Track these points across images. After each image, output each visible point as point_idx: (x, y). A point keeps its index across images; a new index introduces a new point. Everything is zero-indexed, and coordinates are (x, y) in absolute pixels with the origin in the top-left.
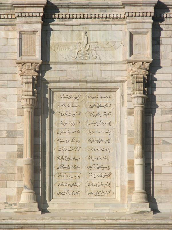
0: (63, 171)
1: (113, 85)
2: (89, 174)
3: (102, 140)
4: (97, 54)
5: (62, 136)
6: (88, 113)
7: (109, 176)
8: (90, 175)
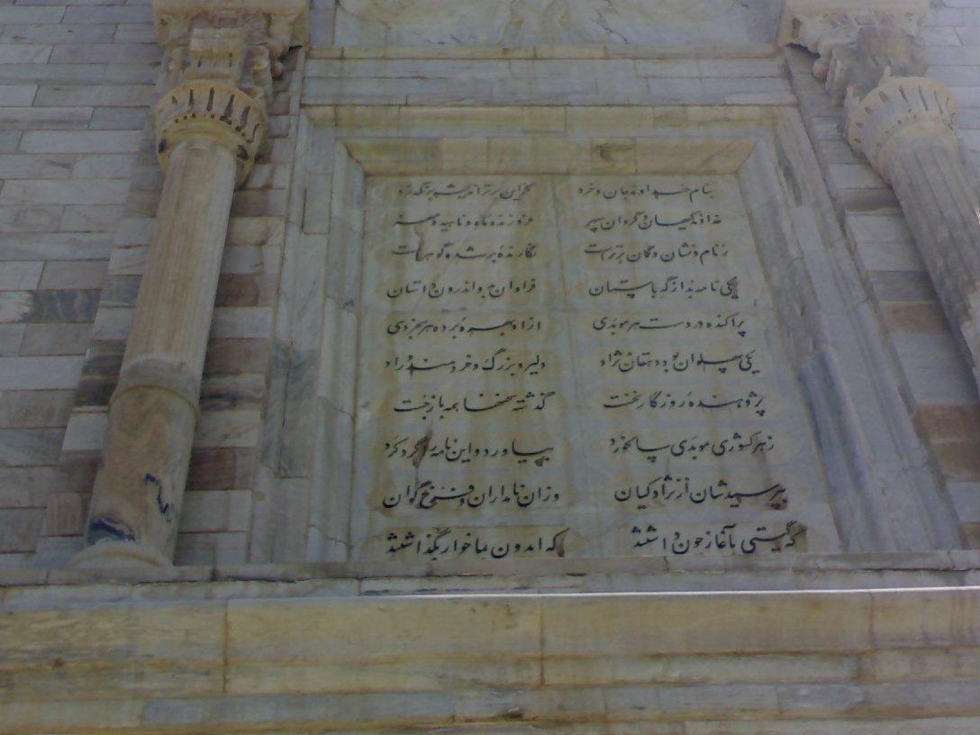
0: (426, 522)
2: (635, 530)
3: (697, 358)
4: (611, 31)
5: (419, 347)
6: (584, 247)
7: (787, 540)
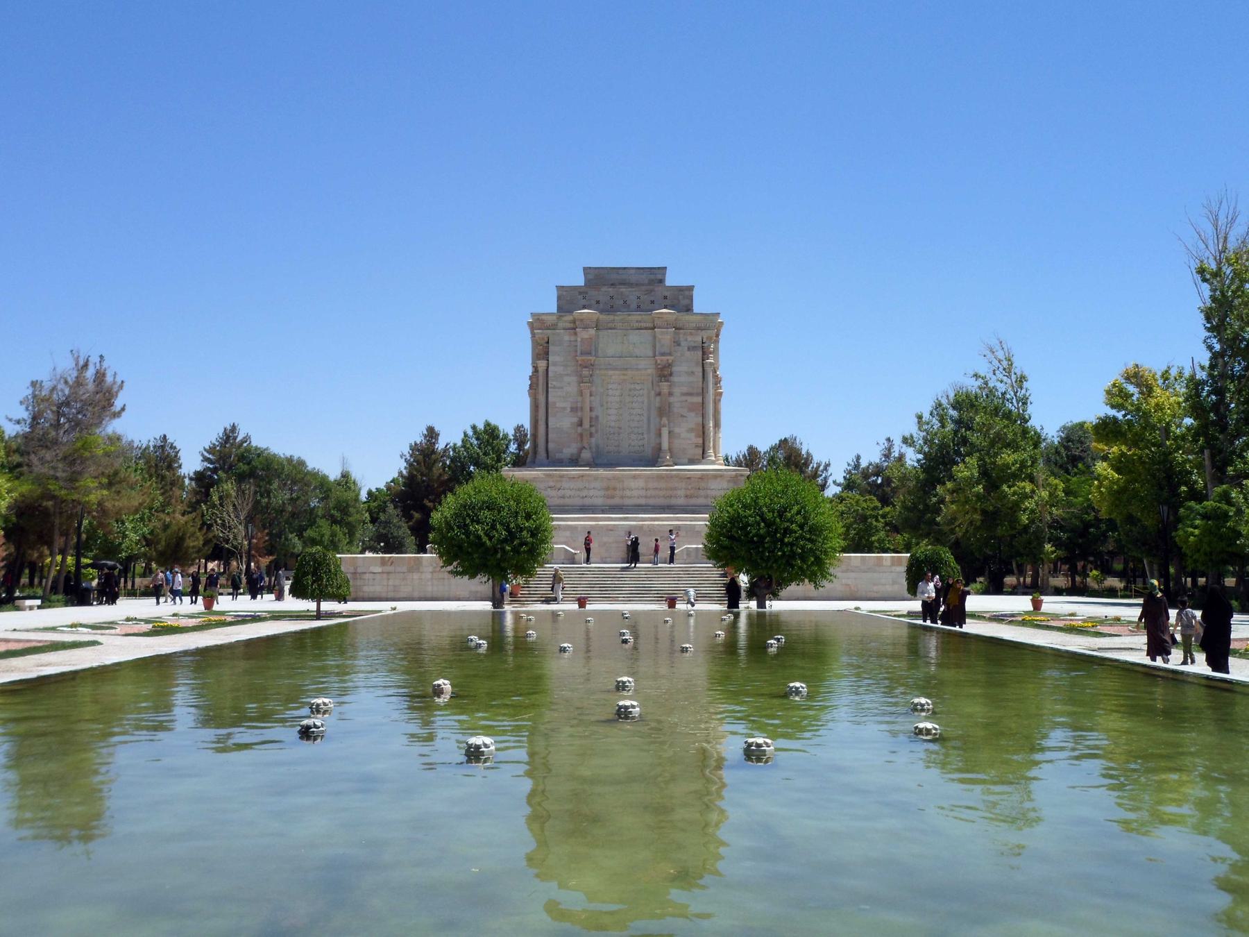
5: (610, 411)
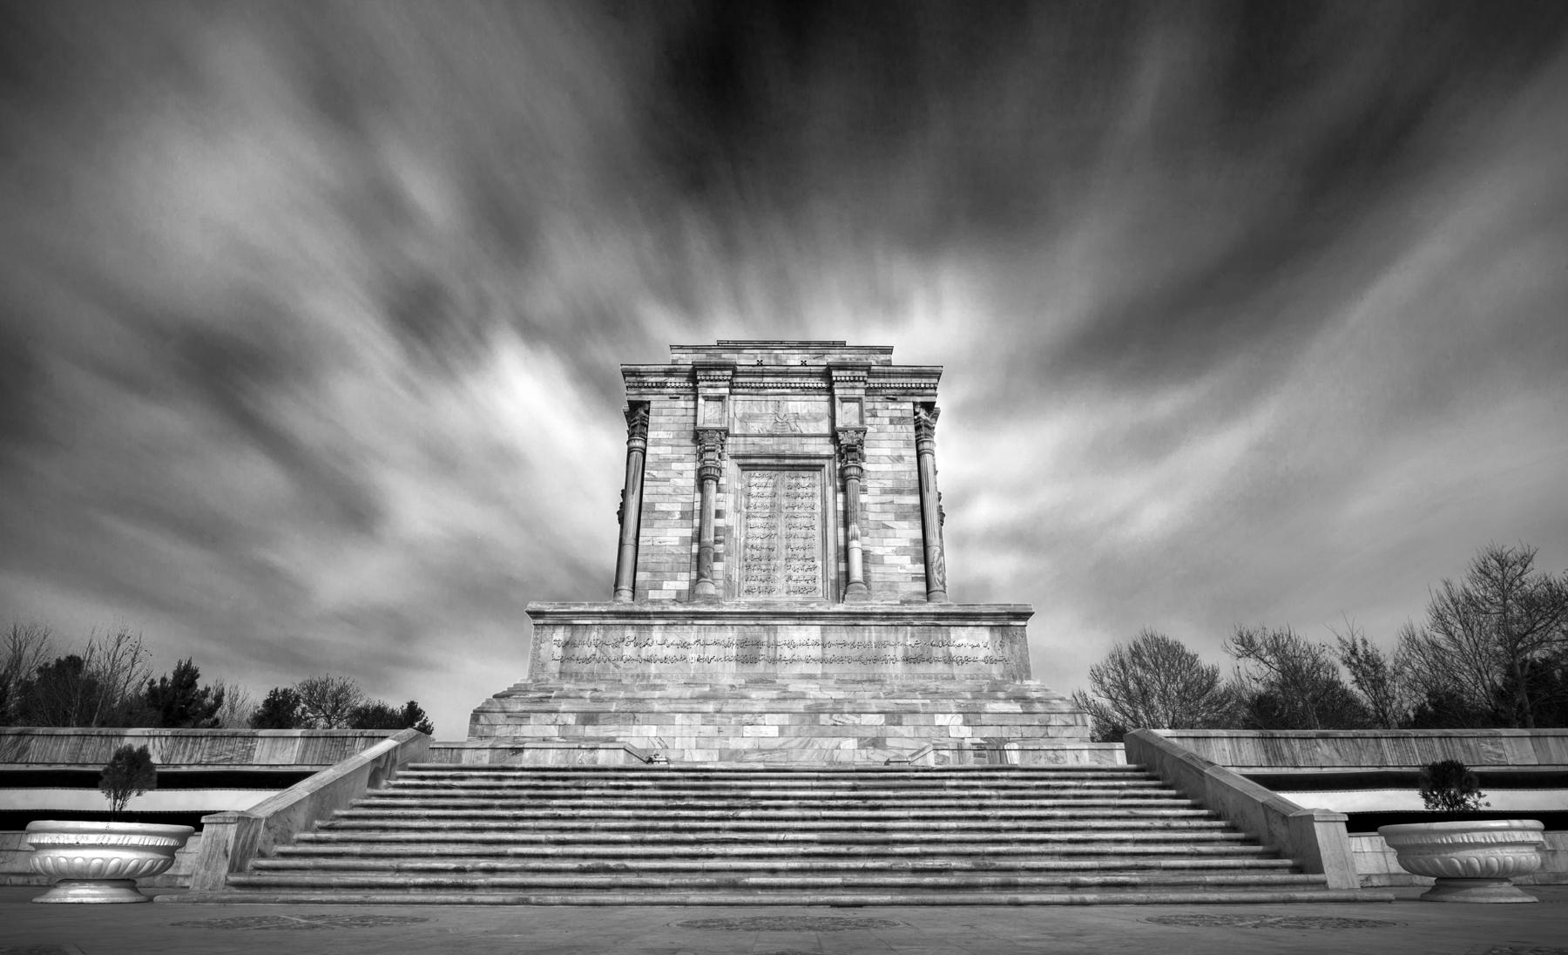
1: (818, 462)
5: (752, 521)
8: (788, 567)
